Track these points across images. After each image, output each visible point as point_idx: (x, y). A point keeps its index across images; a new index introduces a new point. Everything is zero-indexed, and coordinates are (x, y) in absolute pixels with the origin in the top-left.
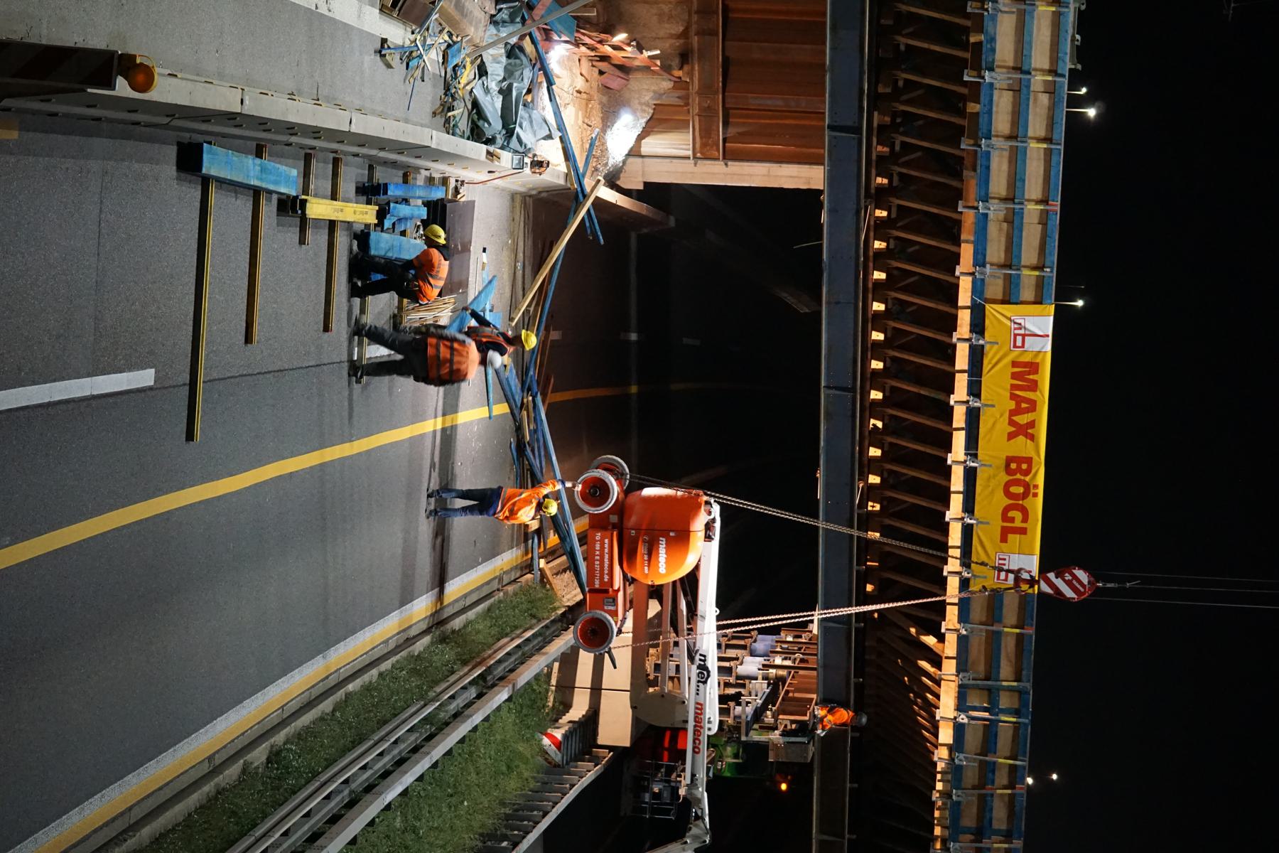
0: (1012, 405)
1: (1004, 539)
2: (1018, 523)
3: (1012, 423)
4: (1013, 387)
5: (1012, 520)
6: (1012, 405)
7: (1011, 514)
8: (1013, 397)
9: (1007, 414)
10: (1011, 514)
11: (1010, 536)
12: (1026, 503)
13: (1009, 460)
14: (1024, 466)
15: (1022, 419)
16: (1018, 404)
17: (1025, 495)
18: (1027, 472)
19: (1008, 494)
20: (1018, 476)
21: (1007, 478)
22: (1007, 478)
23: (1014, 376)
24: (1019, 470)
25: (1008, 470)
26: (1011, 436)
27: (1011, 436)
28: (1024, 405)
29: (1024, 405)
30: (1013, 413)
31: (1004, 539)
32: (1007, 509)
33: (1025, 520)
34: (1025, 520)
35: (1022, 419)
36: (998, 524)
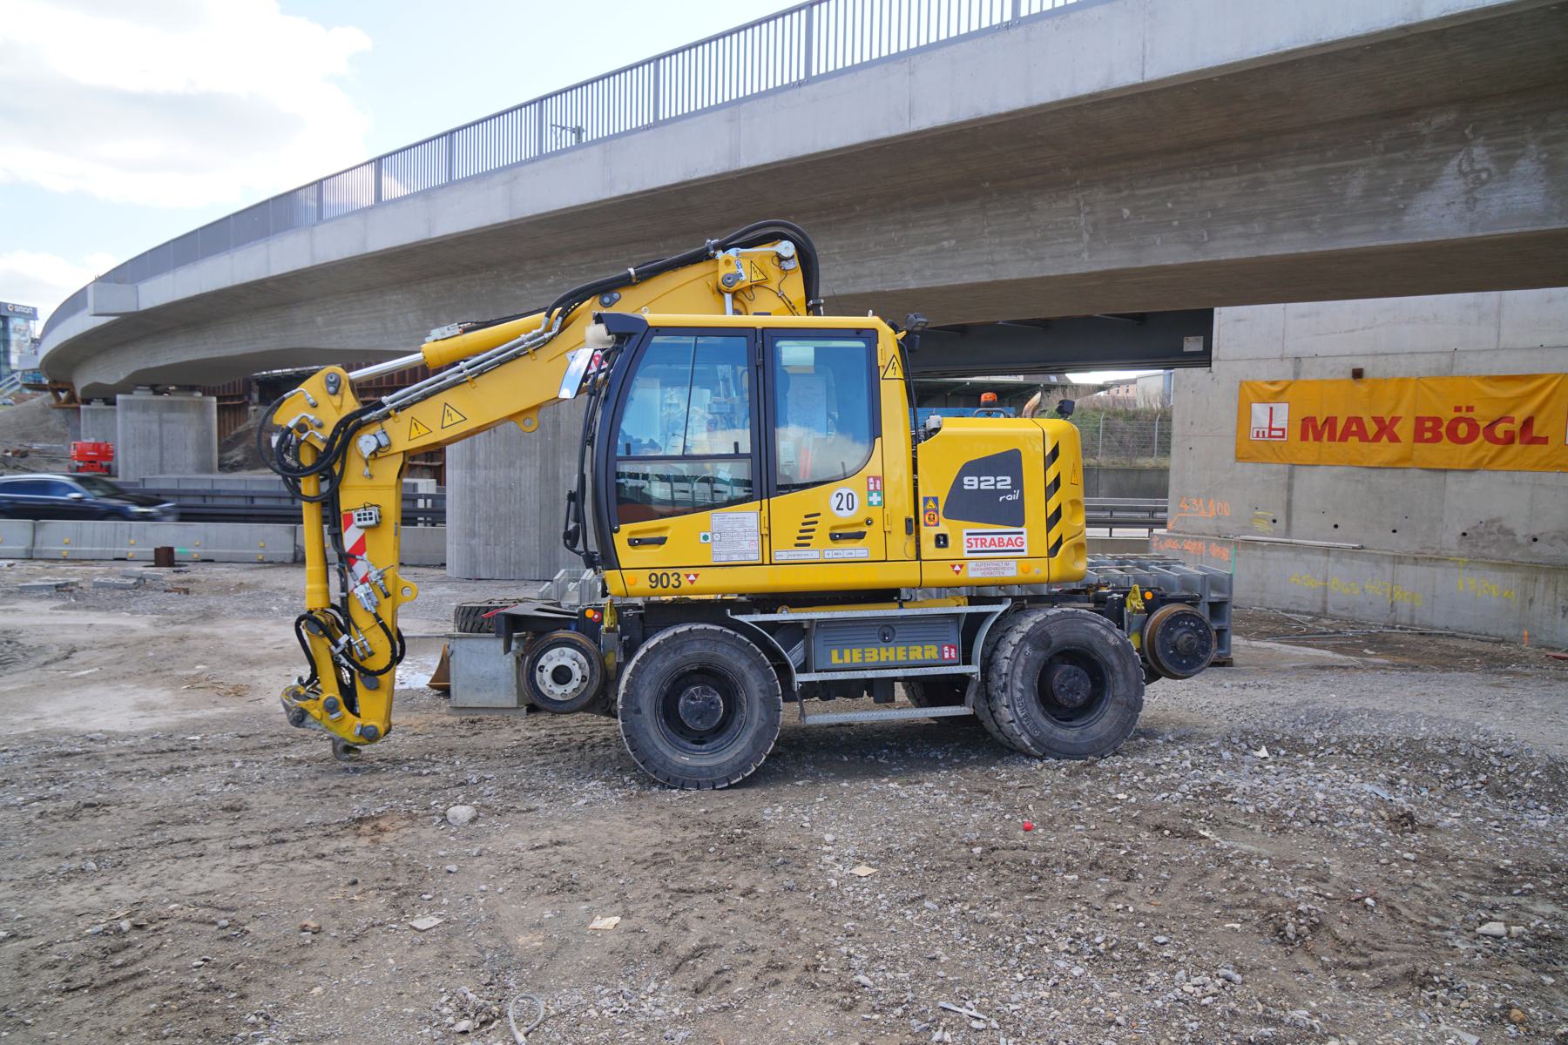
0: (1354, 440)
3: (1377, 438)
4: (1332, 438)
6: (1354, 440)
8: (1344, 438)
12: (1483, 424)
13: (1418, 437)
15: (1372, 429)
16: (1354, 434)
17: (1473, 426)
18: (1437, 421)
19: (1471, 437)
20: (1443, 430)
23: (1318, 437)
25: (1437, 438)
27: (1394, 439)
28: (1354, 428)
29: (1354, 428)
30: (1363, 437)
32: (1495, 440)
35: (1372, 429)
36: (1517, 446)
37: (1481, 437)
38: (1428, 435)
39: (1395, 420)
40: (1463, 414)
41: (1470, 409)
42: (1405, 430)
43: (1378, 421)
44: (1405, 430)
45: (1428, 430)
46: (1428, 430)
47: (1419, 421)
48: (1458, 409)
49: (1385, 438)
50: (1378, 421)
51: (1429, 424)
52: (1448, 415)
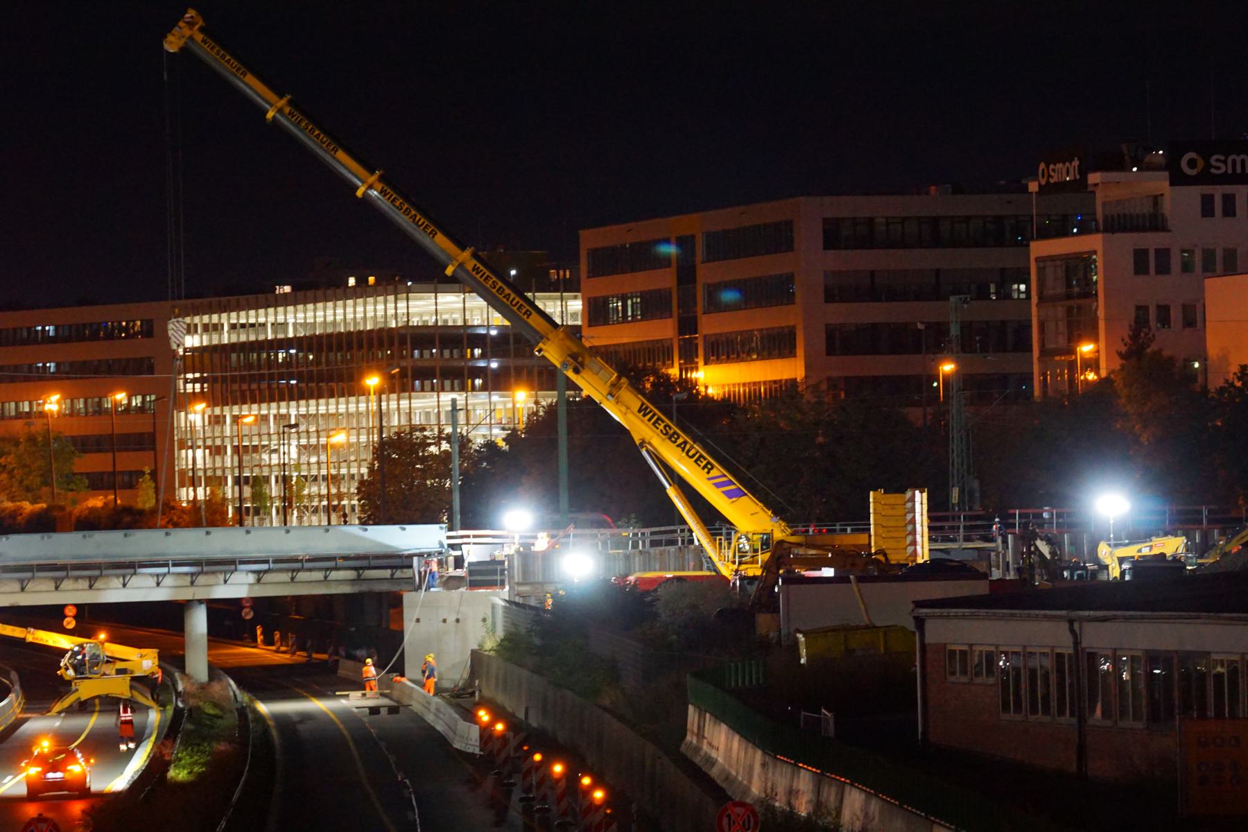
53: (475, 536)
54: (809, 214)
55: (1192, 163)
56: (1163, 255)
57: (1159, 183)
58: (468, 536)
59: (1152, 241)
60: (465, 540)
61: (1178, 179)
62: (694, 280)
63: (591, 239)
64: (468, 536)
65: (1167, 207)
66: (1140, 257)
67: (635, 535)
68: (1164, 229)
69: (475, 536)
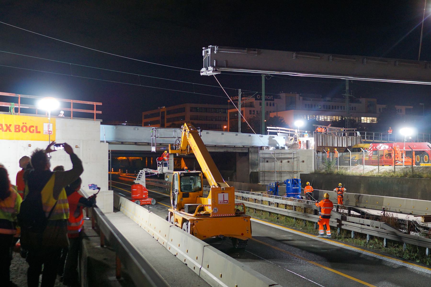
1: (39, 132)
2: (34, 128)
3: (6, 131)
5: (33, 130)
7: (32, 130)
9: (4, 132)
10: (32, 130)
11: (38, 130)
13: (16, 131)
14: (17, 127)
17: (26, 127)
18: (19, 126)
19: (26, 132)
20: (20, 129)
21: (21, 132)
22: (21, 132)
24: (19, 128)
25: (19, 131)
26: (10, 131)
27: (10, 131)
31: (39, 132)
33: (33, 126)
34: (33, 126)
35: (5, 128)
36: (35, 134)
37: (28, 131)
38: (17, 130)
39: (10, 125)
40: (24, 125)
41: (26, 123)
42: (12, 128)
43: (6, 125)
44: (12, 128)
45: (17, 128)
46: (17, 128)
47: (16, 126)
48: (23, 123)
49: (8, 130)
50: (6, 125)
51: (17, 127)
52: (21, 125)
53: (281, 130)
54: (188, 106)
55: (259, 97)
56: (254, 111)
57: (253, 100)
58: (278, 129)
59: (252, 109)
60: (278, 131)
61: (256, 99)
62: (164, 118)
63: (144, 113)
64: (278, 129)
65: (254, 103)
66: (250, 111)
67: (344, 130)
68: (254, 107)
69: (281, 130)
